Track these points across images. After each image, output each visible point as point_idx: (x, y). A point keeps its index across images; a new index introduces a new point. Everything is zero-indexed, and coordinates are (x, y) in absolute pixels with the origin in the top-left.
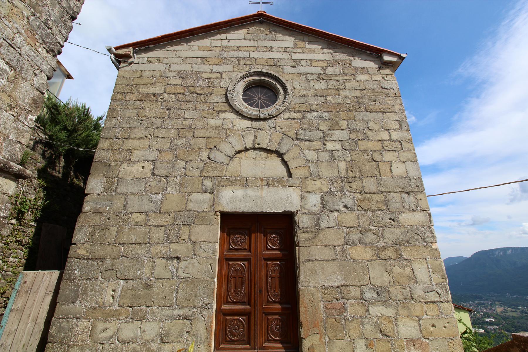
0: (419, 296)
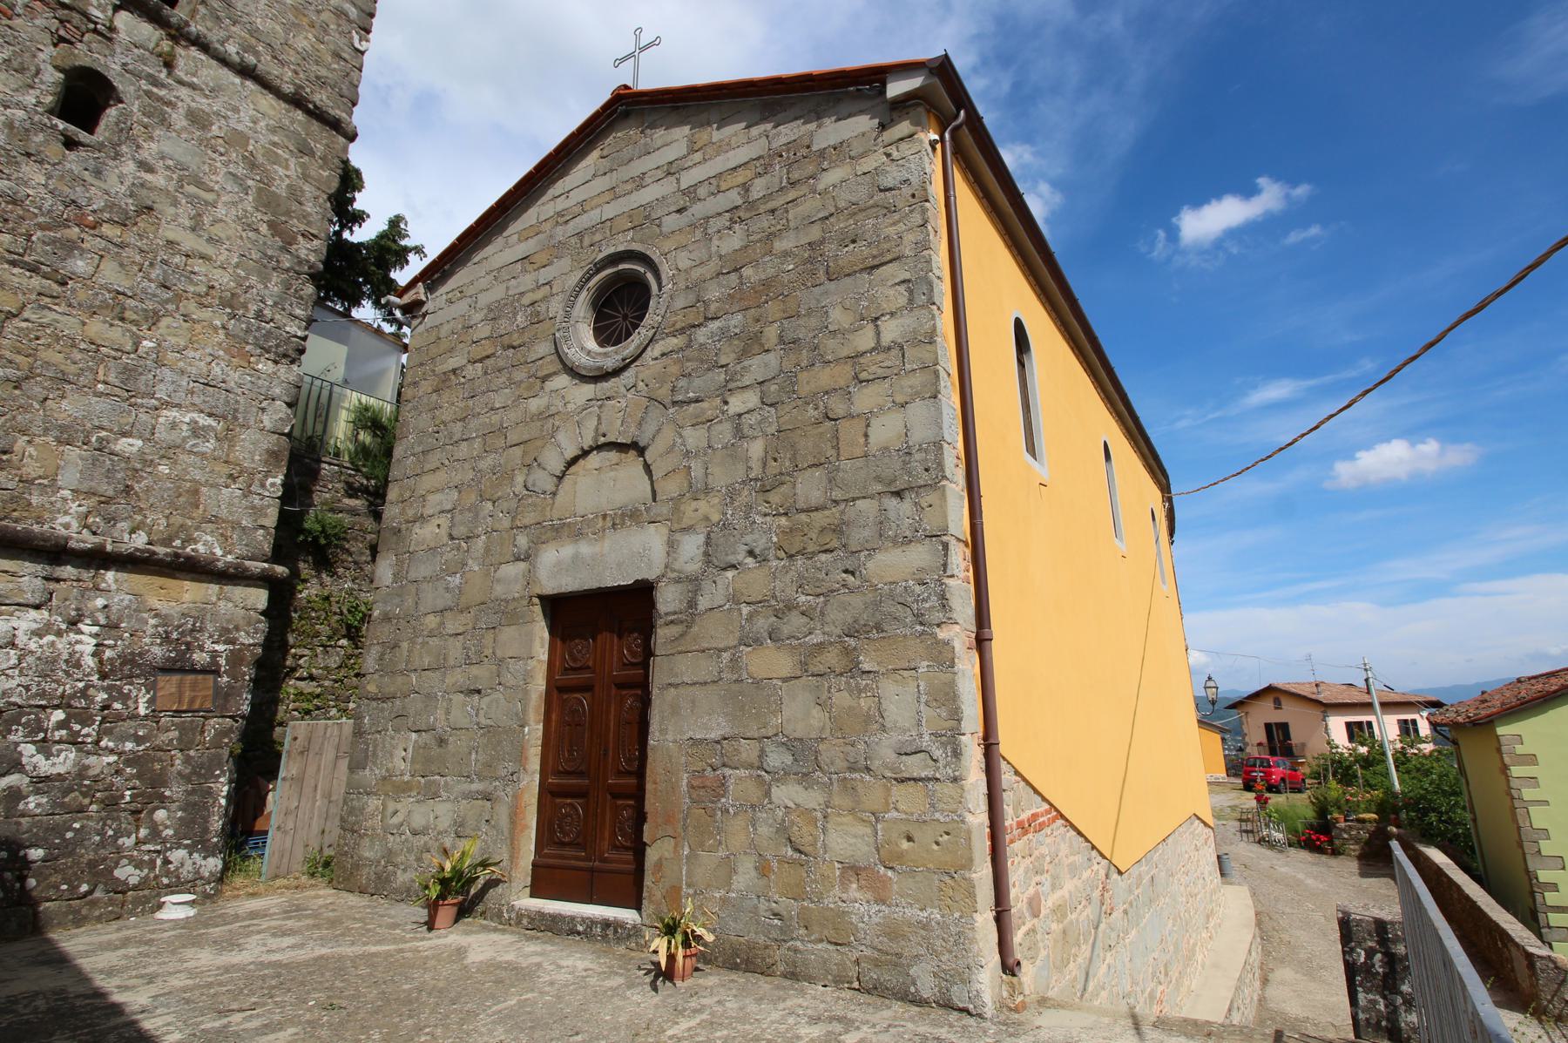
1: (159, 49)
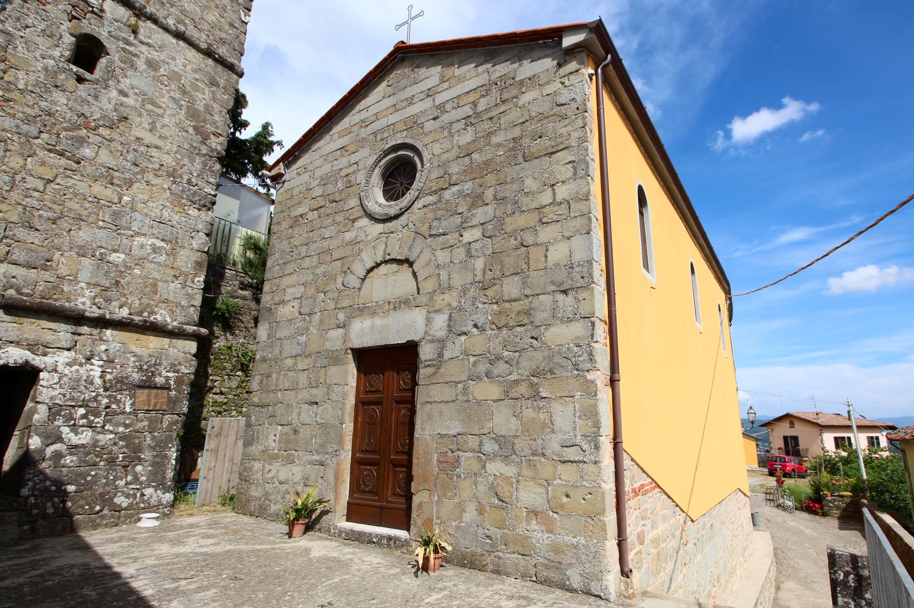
0: (554, 453)
1: (129, 23)
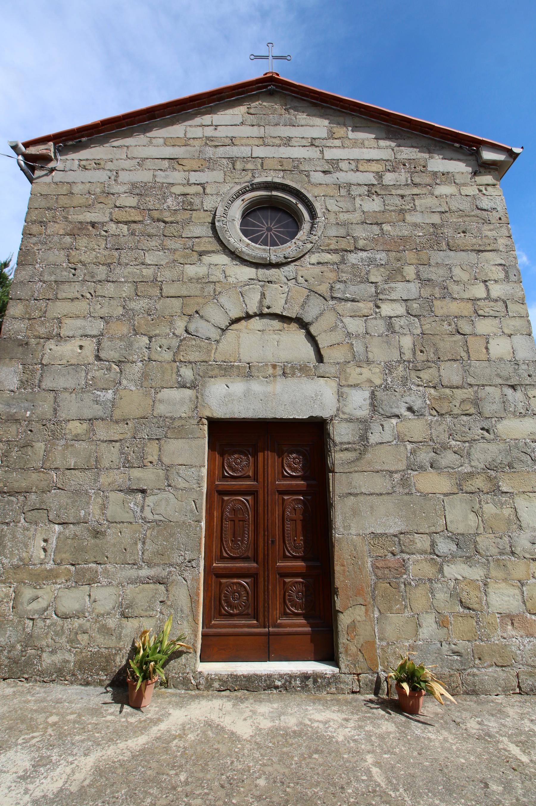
0: (524, 550)
